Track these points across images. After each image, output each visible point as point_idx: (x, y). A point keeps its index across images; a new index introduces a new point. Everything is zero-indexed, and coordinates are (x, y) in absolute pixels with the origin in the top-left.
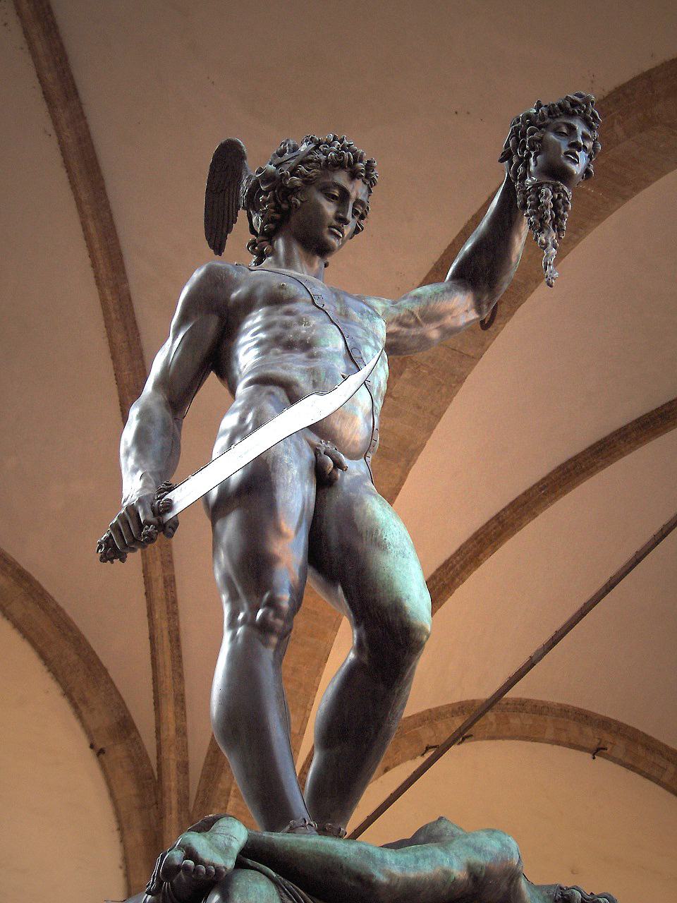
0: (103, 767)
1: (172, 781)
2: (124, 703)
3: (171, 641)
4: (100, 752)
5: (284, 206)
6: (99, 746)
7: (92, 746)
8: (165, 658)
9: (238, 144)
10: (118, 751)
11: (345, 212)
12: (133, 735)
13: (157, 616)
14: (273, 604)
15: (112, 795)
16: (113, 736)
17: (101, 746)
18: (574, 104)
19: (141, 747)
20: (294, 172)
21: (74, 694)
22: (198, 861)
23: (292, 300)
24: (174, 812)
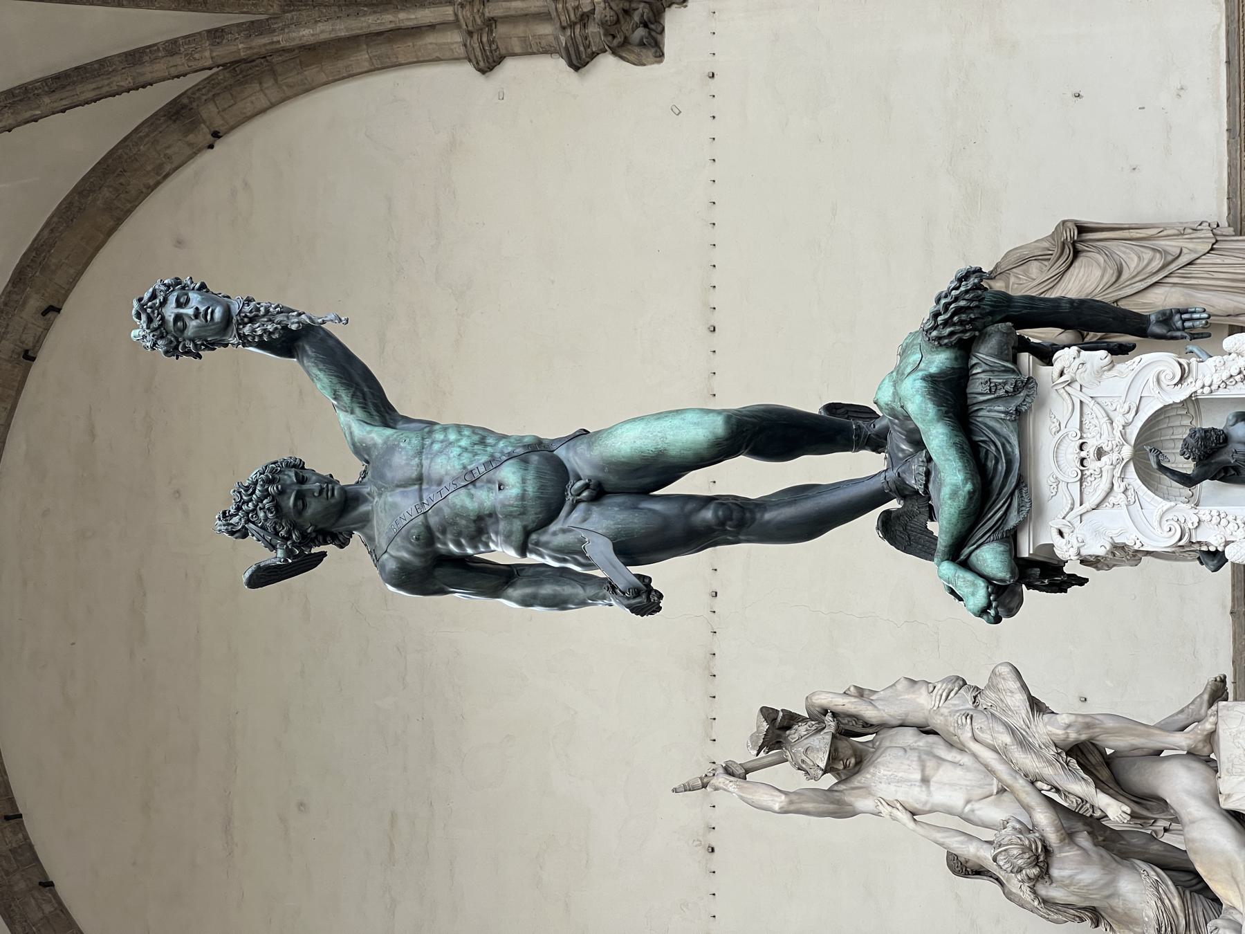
0: (232, 128)
1: (239, 48)
2: (147, 120)
3: (64, 87)
4: (216, 135)
5: (314, 535)
6: (209, 138)
7: (211, 147)
8: (87, 90)
9: (251, 576)
10: (209, 112)
11: (312, 491)
12: (185, 101)
13: (38, 112)
14: (722, 523)
15: (263, 111)
16: (190, 124)
17: (209, 137)
18: (150, 320)
19: (197, 88)
20: (285, 539)
21: (152, 182)
22: (989, 606)
23: (428, 528)
24: (275, 39)
